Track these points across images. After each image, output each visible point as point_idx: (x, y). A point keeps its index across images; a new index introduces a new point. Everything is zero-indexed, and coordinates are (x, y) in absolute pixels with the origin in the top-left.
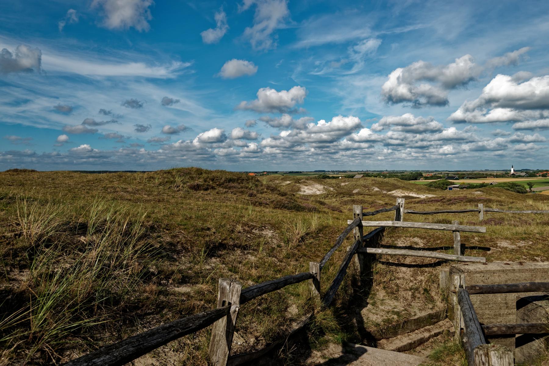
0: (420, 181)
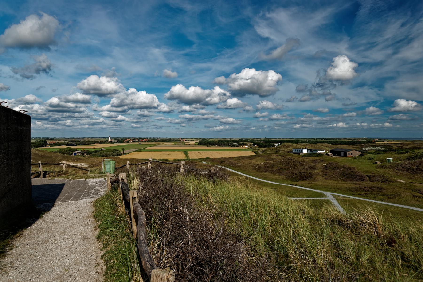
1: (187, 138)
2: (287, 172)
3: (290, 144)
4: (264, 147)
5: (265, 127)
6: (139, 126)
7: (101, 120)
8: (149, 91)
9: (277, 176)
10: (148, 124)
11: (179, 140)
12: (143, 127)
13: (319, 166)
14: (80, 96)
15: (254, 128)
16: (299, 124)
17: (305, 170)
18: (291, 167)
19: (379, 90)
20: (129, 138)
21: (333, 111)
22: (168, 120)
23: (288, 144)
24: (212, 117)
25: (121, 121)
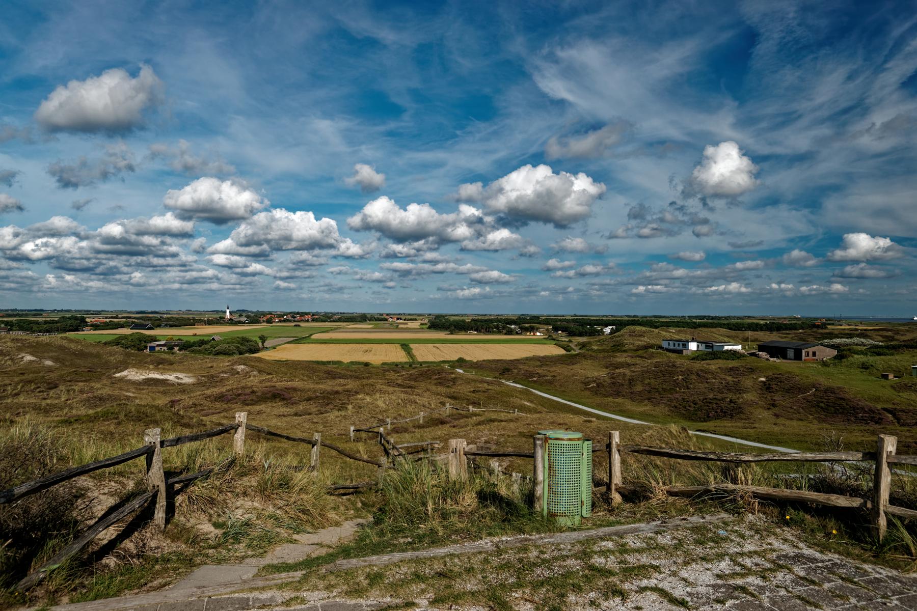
0: (85, 332)
1: (399, 314)
2: (669, 396)
3: (644, 329)
4: (581, 335)
5: (571, 289)
6: (292, 285)
7: (210, 272)
8: (320, 211)
9: (646, 408)
10: (313, 282)
11: (383, 317)
12: (301, 289)
13: (747, 382)
14: (169, 221)
15: (546, 293)
16: (643, 285)
17: (715, 393)
18: (676, 382)
19: (812, 213)
20: (270, 313)
21: (714, 257)
22: (356, 273)
23: (638, 328)
24: (454, 269)
25: (254, 274)
